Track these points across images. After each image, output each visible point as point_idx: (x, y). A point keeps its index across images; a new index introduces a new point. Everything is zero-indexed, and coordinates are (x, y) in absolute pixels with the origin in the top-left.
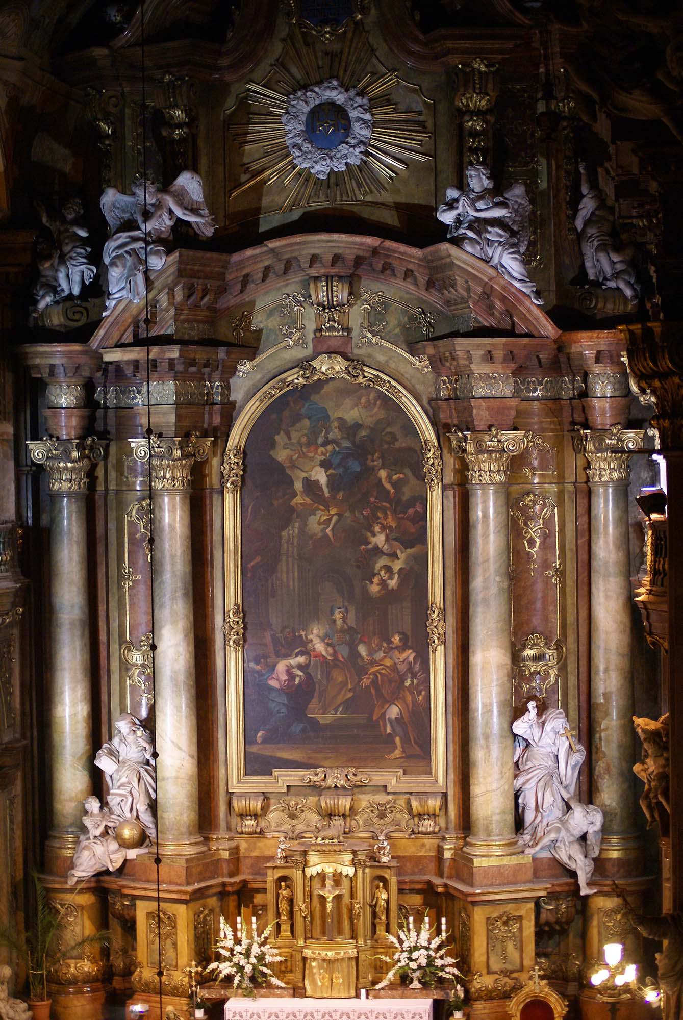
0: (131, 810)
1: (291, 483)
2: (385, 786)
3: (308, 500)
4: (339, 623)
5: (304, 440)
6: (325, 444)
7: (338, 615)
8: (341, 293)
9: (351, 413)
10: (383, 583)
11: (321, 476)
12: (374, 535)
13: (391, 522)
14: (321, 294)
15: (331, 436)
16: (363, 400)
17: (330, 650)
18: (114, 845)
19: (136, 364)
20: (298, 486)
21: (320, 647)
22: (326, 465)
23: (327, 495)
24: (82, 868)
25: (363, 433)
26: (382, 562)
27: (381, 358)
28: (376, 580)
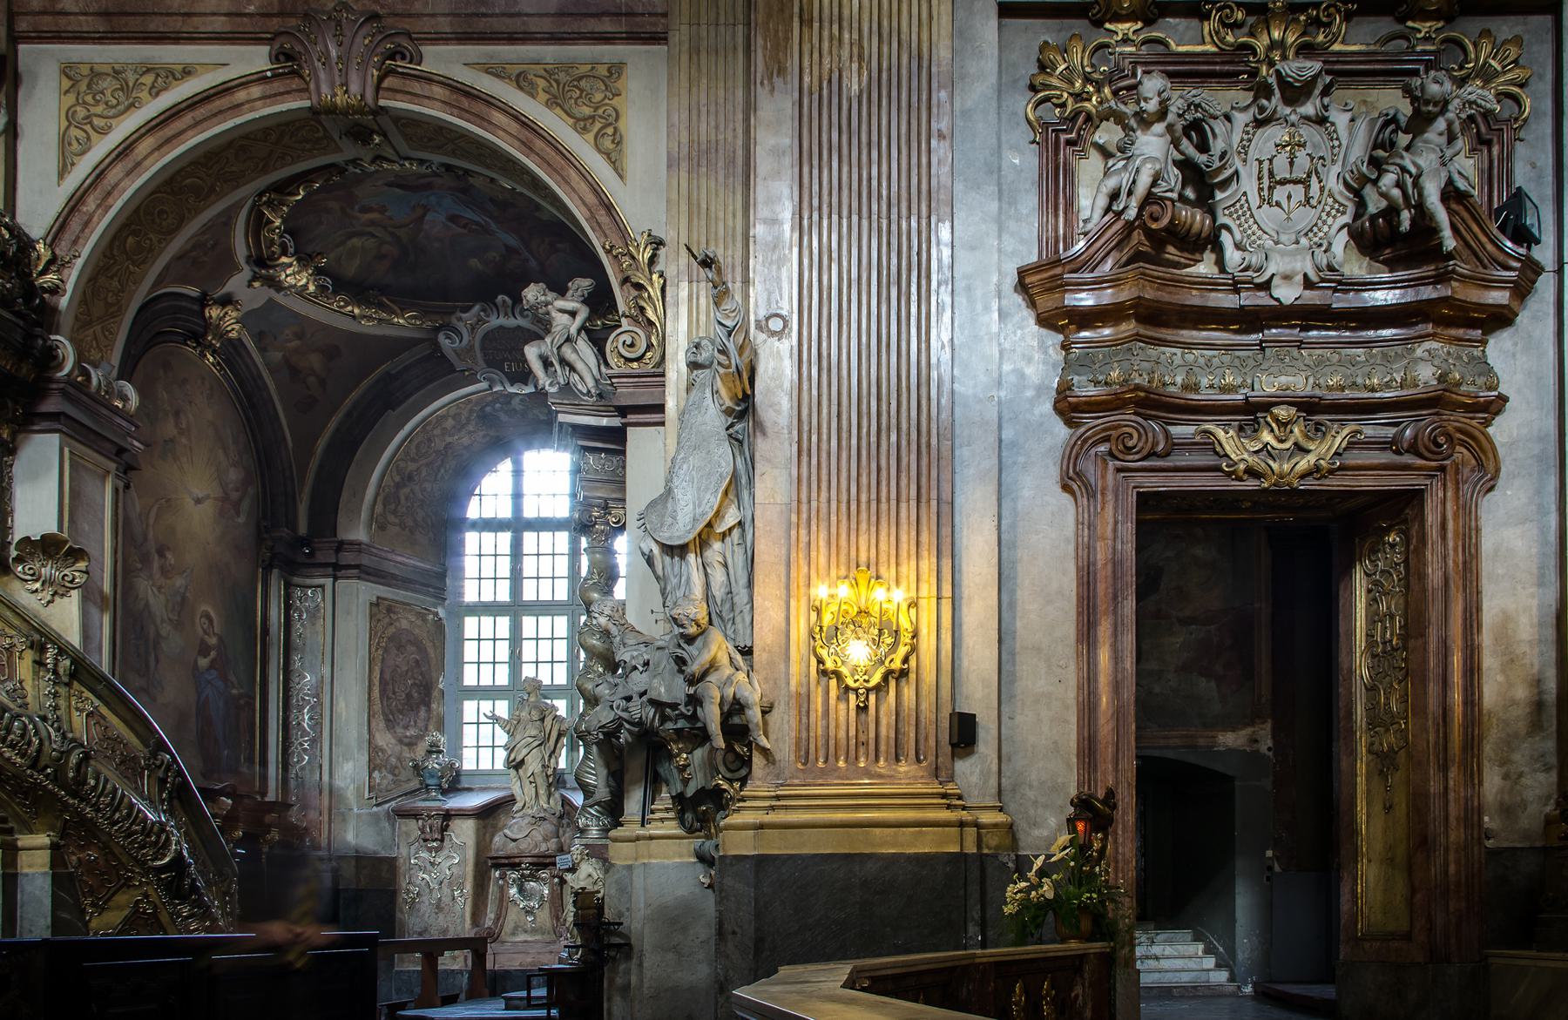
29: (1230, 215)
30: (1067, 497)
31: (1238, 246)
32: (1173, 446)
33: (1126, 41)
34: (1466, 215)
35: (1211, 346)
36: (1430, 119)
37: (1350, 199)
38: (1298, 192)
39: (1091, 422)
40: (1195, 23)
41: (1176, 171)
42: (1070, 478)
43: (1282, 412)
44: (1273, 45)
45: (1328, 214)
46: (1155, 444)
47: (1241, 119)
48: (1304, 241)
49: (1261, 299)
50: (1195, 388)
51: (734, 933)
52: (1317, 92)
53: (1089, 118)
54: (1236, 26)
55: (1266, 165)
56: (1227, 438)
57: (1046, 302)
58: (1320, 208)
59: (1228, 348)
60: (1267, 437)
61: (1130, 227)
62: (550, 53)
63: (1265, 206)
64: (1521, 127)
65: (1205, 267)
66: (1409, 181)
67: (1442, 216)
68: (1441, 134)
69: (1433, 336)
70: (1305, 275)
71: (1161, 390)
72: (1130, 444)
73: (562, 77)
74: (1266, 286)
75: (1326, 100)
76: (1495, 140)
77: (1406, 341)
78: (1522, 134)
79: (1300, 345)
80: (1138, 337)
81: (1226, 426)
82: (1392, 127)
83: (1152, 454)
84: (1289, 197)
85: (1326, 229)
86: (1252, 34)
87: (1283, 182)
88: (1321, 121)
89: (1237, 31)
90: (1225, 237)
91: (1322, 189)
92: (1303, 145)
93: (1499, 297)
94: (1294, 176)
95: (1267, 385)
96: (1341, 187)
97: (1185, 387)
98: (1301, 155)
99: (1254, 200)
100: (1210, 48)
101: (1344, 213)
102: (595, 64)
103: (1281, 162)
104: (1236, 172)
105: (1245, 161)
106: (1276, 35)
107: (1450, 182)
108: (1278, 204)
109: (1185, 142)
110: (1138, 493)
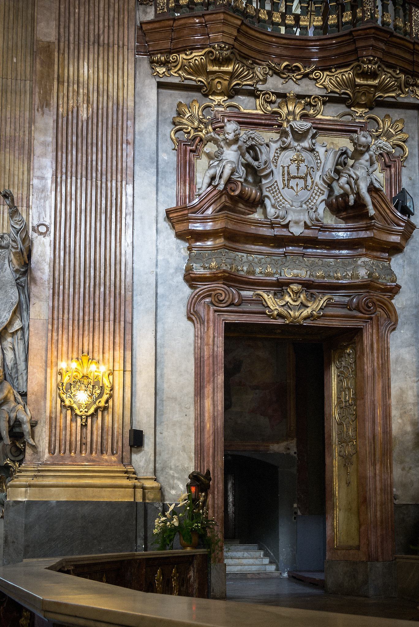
29: (269, 191)
30: (190, 324)
31: (273, 206)
32: (242, 301)
33: (219, 105)
34: (379, 199)
35: (261, 253)
36: (362, 153)
37: (325, 188)
38: (301, 183)
39: (203, 287)
40: (252, 99)
41: (243, 169)
42: (191, 314)
43: (295, 287)
44: (289, 113)
45: (316, 194)
46: (233, 299)
47: (274, 146)
48: (304, 206)
49: (284, 232)
50: (253, 273)
51: (13, 542)
52: (309, 137)
53: (201, 140)
54: (271, 102)
55: (286, 168)
57: (181, 227)
58: (312, 191)
59: (269, 255)
61: (221, 193)
63: (286, 188)
64: (404, 161)
65: (257, 216)
66: (353, 181)
67: (368, 199)
68: (367, 161)
69: (365, 255)
70: (305, 222)
71: (236, 273)
72: (221, 298)
74: (287, 226)
75: (314, 141)
76: (393, 165)
77: (352, 257)
78: (405, 164)
79: (303, 255)
80: (225, 247)
81: (268, 292)
82: (345, 156)
83: (232, 304)
84: (297, 185)
85: (315, 201)
86: (279, 107)
87: (294, 177)
89: (272, 105)
90: (267, 202)
91: (313, 182)
92: (303, 161)
93: (395, 239)
94: (299, 175)
95: (288, 274)
96: (322, 182)
97: (248, 272)
98: (302, 165)
99: (281, 185)
100: (260, 112)
101: (323, 194)
103: (293, 168)
104: (272, 171)
105: (276, 166)
106: (291, 108)
107: (372, 183)
108: (292, 188)
109: (247, 155)
110: (225, 323)
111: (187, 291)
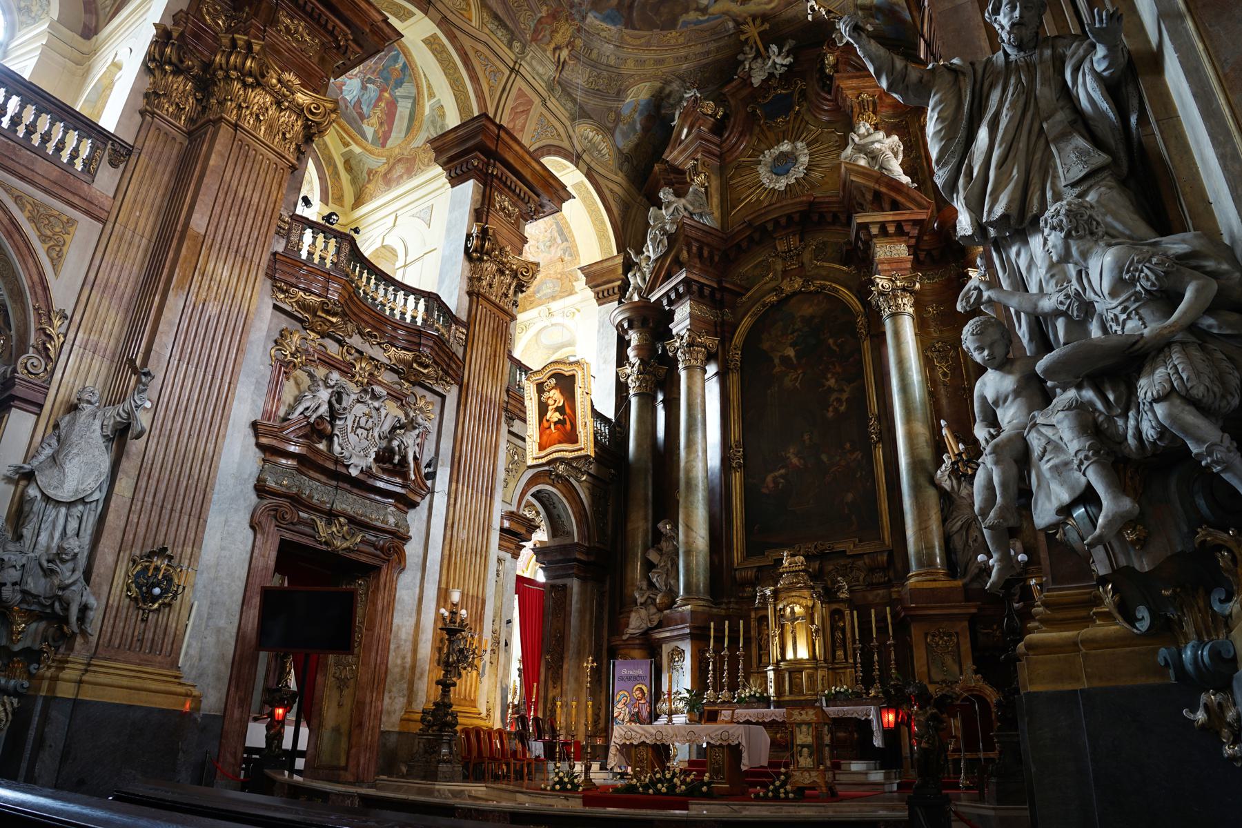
0: (666, 585)
1: (773, 361)
2: (845, 551)
3: (783, 368)
4: (807, 442)
5: (779, 333)
6: (792, 333)
7: (806, 437)
8: (794, 241)
9: (807, 310)
10: (836, 410)
11: (791, 352)
12: (828, 380)
13: (838, 369)
14: (781, 247)
15: (796, 327)
16: (816, 301)
17: (802, 461)
18: (653, 610)
19: (667, 294)
20: (777, 361)
21: (795, 460)
22: (793, 345)
23: (795, 362)
24: (631, 626)
25: (816, 320)
26: (834, 396)
27: (824, 273)
28: (831, 409)
30: (250, 533)
31: (339, 445)
35: (318, 481)
39: (269, 502)
47: (354, 397)
49: (344, 471)
53: (295, 365)
56: (321, 525)
60: (334, 529)
62: (40, 195)
73: (41, 210)
74: (348, 467)
81: (321, 519)
88: (378, 410)
90: (336, 439)
97: (308, 496)
98: (370, 420)
102: (61, 213)
111: (253, 498)
